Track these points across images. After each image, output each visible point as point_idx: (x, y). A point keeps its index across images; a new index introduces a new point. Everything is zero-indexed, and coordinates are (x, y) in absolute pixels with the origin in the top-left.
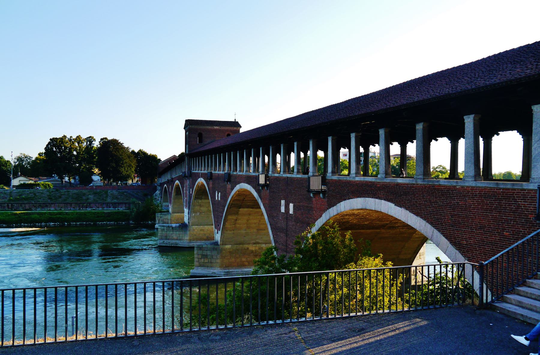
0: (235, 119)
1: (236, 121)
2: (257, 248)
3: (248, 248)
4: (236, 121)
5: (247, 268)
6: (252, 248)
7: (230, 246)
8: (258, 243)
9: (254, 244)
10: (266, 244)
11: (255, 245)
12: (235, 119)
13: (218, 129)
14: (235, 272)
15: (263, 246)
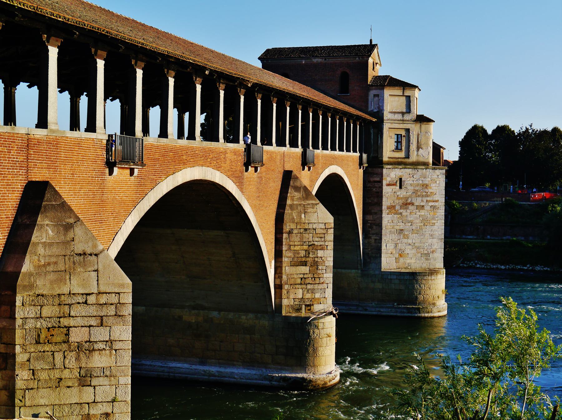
0: (371, 40)
1: (373, 43)
2: (200, 319)
3: (180, 318)
4: (373, 43)
5: (179, 361)
6: (190, 317)
7: (144, 308)
8: (203, 308)
9: (194, 308)
10: (220, 310)
11: (196, 311)
12: (371, 40)
13: (321, 63)
14: (147, 367)
15: (215, 314)
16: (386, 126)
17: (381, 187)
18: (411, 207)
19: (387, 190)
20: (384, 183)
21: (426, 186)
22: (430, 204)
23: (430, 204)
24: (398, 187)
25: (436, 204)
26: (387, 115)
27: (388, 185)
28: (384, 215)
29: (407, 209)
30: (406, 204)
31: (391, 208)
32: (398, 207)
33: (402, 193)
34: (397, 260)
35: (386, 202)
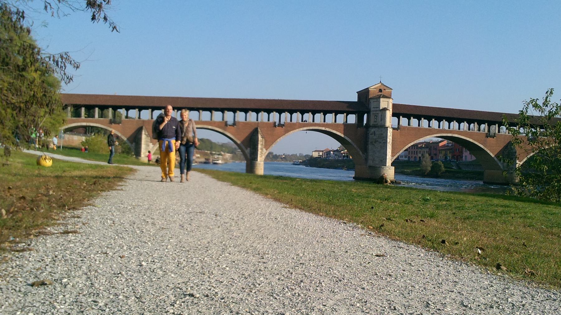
16: (371, 113)
17: (369, 135)
18: (377, 142)
19: (370, 136)
20: (370, 134)
21: (382, 134)
22: (383, 141)
23: (383, 141)
24: (373, 135)
25: (385, 141)
26: (372, 109)
27: (371, 134)
28: (369, 146)
29: (376, 143)
30: (376, 142)
31: (372, 143)
32: (373, 143)
33: (375, 137)
34: (373, 162)
35: (370, 141)
